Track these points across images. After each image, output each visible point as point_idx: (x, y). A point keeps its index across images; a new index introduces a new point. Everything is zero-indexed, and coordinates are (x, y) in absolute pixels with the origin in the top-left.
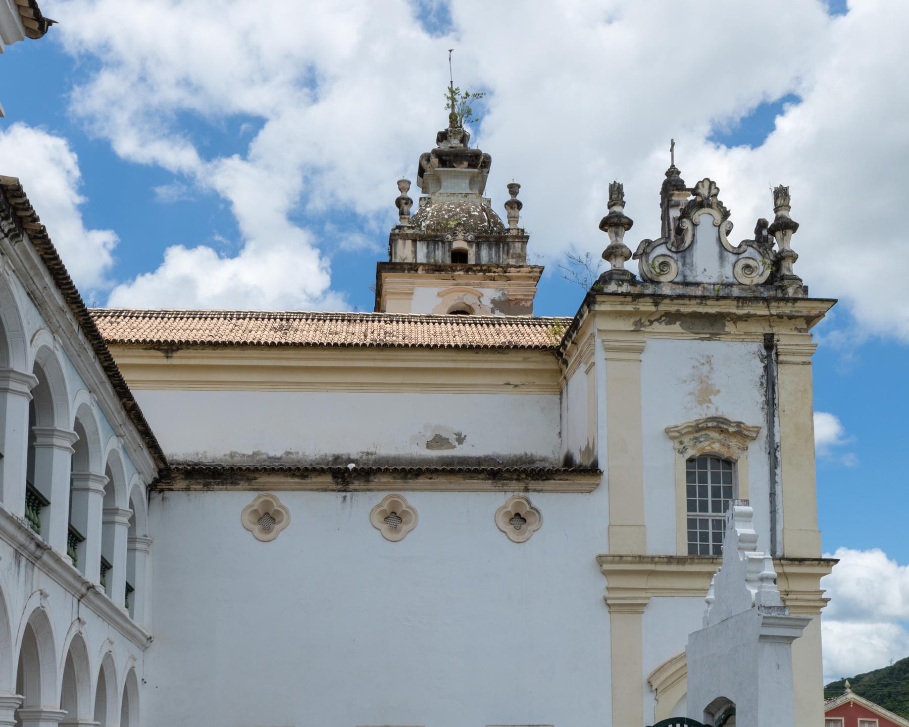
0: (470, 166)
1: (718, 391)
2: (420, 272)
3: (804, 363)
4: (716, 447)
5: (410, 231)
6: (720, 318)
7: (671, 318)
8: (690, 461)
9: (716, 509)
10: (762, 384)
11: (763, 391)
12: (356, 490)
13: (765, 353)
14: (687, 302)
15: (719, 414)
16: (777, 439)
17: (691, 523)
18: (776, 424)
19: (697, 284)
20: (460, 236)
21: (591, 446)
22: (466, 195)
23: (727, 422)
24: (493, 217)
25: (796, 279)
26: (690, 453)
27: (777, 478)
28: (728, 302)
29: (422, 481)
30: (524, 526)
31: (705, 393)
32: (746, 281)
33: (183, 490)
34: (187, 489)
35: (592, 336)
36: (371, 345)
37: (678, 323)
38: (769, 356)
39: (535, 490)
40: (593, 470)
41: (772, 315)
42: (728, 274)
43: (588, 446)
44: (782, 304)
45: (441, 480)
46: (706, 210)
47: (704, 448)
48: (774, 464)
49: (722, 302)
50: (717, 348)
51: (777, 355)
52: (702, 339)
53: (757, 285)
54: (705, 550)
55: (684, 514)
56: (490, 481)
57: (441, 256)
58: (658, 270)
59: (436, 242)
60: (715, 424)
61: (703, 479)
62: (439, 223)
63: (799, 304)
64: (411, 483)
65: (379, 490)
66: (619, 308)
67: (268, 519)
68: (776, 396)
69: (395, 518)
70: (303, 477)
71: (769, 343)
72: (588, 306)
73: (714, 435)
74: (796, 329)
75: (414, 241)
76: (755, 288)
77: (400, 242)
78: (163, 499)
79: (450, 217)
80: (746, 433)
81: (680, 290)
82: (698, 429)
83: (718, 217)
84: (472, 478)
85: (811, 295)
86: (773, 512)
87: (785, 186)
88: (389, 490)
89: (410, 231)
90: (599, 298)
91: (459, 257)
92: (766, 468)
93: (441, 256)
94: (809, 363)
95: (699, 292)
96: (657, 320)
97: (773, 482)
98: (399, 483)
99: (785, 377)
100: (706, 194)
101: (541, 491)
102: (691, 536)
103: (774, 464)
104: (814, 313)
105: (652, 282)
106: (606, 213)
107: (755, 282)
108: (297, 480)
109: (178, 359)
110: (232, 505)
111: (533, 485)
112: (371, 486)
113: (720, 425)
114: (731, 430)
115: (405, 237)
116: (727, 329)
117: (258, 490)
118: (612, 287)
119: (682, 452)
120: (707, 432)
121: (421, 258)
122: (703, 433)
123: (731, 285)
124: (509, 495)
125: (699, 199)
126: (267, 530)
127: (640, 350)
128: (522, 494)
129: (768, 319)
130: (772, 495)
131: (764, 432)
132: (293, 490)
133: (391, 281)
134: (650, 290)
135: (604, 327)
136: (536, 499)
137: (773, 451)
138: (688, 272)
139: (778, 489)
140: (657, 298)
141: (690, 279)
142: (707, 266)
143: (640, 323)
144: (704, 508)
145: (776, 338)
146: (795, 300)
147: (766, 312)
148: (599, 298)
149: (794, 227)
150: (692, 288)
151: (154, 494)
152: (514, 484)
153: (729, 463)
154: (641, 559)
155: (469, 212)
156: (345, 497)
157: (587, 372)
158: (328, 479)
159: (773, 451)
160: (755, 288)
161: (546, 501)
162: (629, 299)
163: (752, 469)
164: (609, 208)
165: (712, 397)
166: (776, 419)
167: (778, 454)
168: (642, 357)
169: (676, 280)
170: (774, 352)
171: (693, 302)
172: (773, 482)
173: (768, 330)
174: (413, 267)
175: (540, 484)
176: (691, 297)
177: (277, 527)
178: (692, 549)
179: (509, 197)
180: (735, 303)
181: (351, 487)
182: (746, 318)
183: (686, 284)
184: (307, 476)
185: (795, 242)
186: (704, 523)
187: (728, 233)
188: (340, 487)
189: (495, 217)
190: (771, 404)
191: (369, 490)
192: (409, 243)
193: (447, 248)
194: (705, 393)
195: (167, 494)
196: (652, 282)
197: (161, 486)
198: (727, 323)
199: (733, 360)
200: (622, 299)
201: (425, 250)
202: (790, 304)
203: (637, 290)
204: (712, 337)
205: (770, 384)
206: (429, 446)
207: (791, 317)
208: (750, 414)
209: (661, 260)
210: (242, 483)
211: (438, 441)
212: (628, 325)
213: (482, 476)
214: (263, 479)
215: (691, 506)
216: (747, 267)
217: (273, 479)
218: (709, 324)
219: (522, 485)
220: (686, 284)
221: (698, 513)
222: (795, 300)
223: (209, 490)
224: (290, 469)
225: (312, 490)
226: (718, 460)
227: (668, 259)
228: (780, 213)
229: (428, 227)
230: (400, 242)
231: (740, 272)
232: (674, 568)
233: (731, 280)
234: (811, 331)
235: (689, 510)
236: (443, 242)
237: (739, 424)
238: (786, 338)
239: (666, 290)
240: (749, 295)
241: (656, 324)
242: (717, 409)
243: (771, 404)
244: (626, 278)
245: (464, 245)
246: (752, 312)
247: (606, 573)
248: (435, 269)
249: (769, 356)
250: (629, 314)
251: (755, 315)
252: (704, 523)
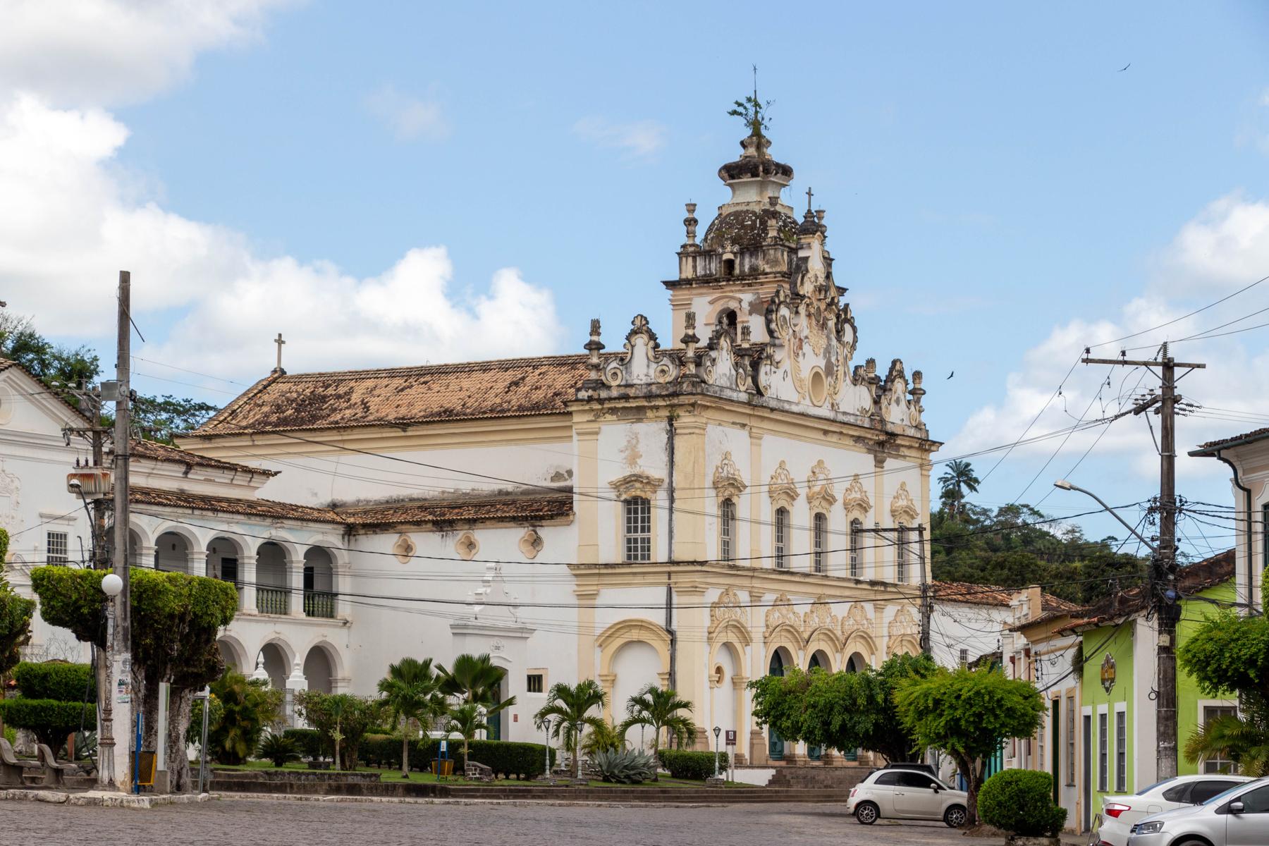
0: (753, 176)
4: (639, 493)
7: (613, 411)
8: (627, 502)
9: (643, 531)
17: (629, 541)
19: (632, 386)
20: (729, 249)
26: (624, 497)
29: (488, 523)
31: (633, 459)
32: (661, 380)
48: (672, 500)
50: (641, 428)
54: (636, 557)
57: (714, 267)
59: (711, 256)
61: (636, 512)
71: (671, 420)
73: (638, 485)
81: (622, 391)
82: (628, 481)
91: (730, 264)
93: (714, 267)
99: (678, 441)
102: (629, 549)
103: (672, 500)
109: (411, 432)
113: (637, 478)
127: (597, 433)
129: (672, 406)
130: (671, 520)
131: (667, 481)
137: (671, 491)
141: (630, 382)
143: (598, 415)
144: (636, 531)
154: (589, 566)
158: (430, 526)
159: (671, 491)
165: (638, 461)
168: (599, 437)
178: (629, 557)
182: (657, 408)
192: (690, 259)
194: (633, 459)
204: (640, 420)
206: (552, 480)
211: (557, 476)
215: (629, 530)
216: (663, 371)
232: (610, 571)
245: (731, 256)
247: (576, 575)
252: (636, 540)
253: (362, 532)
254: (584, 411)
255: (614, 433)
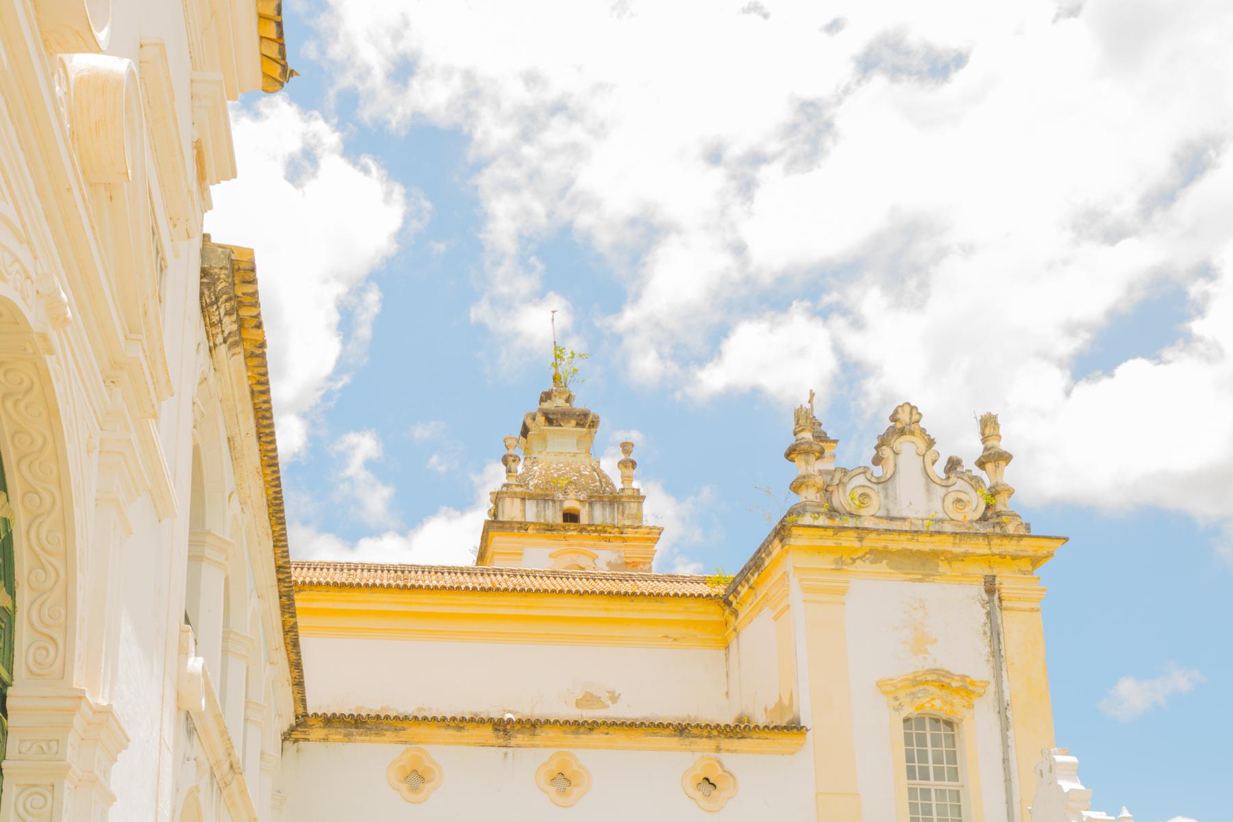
1: (935, 640)
2: (530, 531)
3: (1032, 610)
5: (519, 489)
6: (935, 555)
7: (878, 555)
8: (906, 720)
9: (939, 775)
10: (985, 633)
11: (987, 641)
12: (519, 746)
13: (986, 597)
14: (895, 536)
15: (938, 666)
16: (1007, 697)
18: (1005, 678)
19: (904, 519)
20: (572, 495)
21: (786, 702)
22: (575, 455)
23: (949, 674)
24: (603, 477)
25: (1014, 516)
27: (1010, 742)
28: (943, 537)
29: (596, 736)
30: (714, 792)
33: (320, 740)
34: (325, 740)
35: (785, 575)
36: (514, 589)
37: (885, 562)
38: (990, 601)
39: (728, 750)
40: (795, 727)
41: (993, 555)
42: (937, 509)
43: (780, 705)
44: (1005, 541)
45: (619, 737)
46: (907, 437)
47: (922, 706)
48: (1005, 725)
49: (936, 538)
51: (1000, 600)
52: (913, 580)
53: (971, 521)
55: (904, 783)
56: (676, 739)
58: (857, 503)
60: (935, 677)
61: (922, 741)
62: (547, 483)
63: (1025, 542)
64: (585, 738)
65: (545, 746)
66: (819, 543)
67: (416, 778)
68: (1002, 646)
69: (562, 780)
70: (460, 728)
71: (991, 587)
72: (781, 540)
73: (933, 689)
74: (1020, 571)
75: (523, 499)
76: (968, 525)
77: (508, 501)
78: (298, 750)
79: (559, 476)
80: (971, 687)
81: (884, 525)
83: (922, 446)
84: (655, 734)
85: (1033, 533)
86: (1008, 780)
87: (994, 413)
88: (557, 746)
89: (519, 489)
90: (795, 531)
92: (996, 730)
94: (1038, 610)
95: (906, 526)
96: (860, 558)
97: (1006, 746)
98: (570, 738)
99: (1013, 626)
100: (908, 420)
101: (735, 751)
103: (1005, 725)
104: (1041, 553)
105: (851, 515)
106: (792, 440)
107: (968, 518)
108: (451, 732)
110: (377, 757)
111: (725, 743)
112: (537, 740)
114: (954, 684)
115: (514, 495)
116: (941, 570)
117: (406, 742)
118: (807, 519)
119: (897, 710)
120: (925, 686)
121: (531, 516)
122: (921, 687)
123: (942, 521)
124: (699, 755)
125: (899, 425)
126: (414, 789)
127: (843, 592)
128: (713, 754)
129: (987, 559)
130: (1005, 760)
131: (992, 688)
132: (446, 744)
133: (500, 541)
134: (851, 523)
135: (794, 564)
136: (728, 760)
137: (1003, 710)
138: (891, 506)
139: (1012, 755)
140: (862, 532)
141: (894, 513)
142: (914, 498)
143: (842, 562)
144: (925, 777)
145: (998, 580)
146: (1021, 537)
147: (986, 551)
148: (795, 531)
149: (1006, 457)
150: (899, 523)
151: (288, 744)
152: (704, 743)
153: (949, 724)
155: (579, 471)
156: (506, 754)
157: (776, 618)
158: (488, 731)
160: (968, 525)
161: (740, 760)
162: (830, 532)
163: (978, 729)
164: (795, 434)
166: (1004, 673)
167: (1008, 713)
169: (879, 514)
170: (996, 596)
171: (903, 537)
172: (1006, 746)
173: (988, 572)
174: (523, 526)
175: (735, 743)
176: (900, 532)
177: (427, 786)
179: (622, 457)
180: (951, 539)
181: (513, 742)
182: (963, 557)
183: (892, 519)
184: (463, 728)
185: (1009, 475)
186: (926, 793)
187: (933, 463)
188: (500, 741)
189: (606, 477)
190: (997, 654)
191: (533, 746)
193: (558, 507)
195: (302, 744)
196: (851, 515)
197: (295, 735)
198: (941, 563)
199: (952, 604)
200: (821, 532)
201: (535, 510)
202: (1014, 542)
203: (837, 522)
205: (995, 634)
207: (1014, 558)
208: (977, 667)
209: (861, 491)
210: (388, 733)
212: (826, 562)
213: (667, 732)
214: (413, 731)
215: (911, 773)
216: (959, 501)
217: (423, 730)
218: (923, 563)
219: (713, 743)
220: (892, 519)
221: (918, 781)
222: (1021, 537)
223: (350, 741)
224: (444, 719)
225: (468, 744)
226: (937, 721)
227: (867, 491)
228: (989, 444)
229: (536, 486)
230: (508, 501)
231: (950, 506)
233: (941, 515)
234: (1037, 572)
235: (909, 778)
236: (553, 501)
237: (963, 677)
238: (1009, 582)
239: (868, 524)
240: (963, 530)
241: (859, 562)
242: (935, 661)
243: (997, 654)
244: (822, 510)
245: (577, 505)
246: (971, 550)
248: (550, 528)
249: (990, 601)
250: (829, 550)
251: (973, 554)
252: (926, 793)
253: (318, 732)
254: (819, 550)
255: (877, 595)
